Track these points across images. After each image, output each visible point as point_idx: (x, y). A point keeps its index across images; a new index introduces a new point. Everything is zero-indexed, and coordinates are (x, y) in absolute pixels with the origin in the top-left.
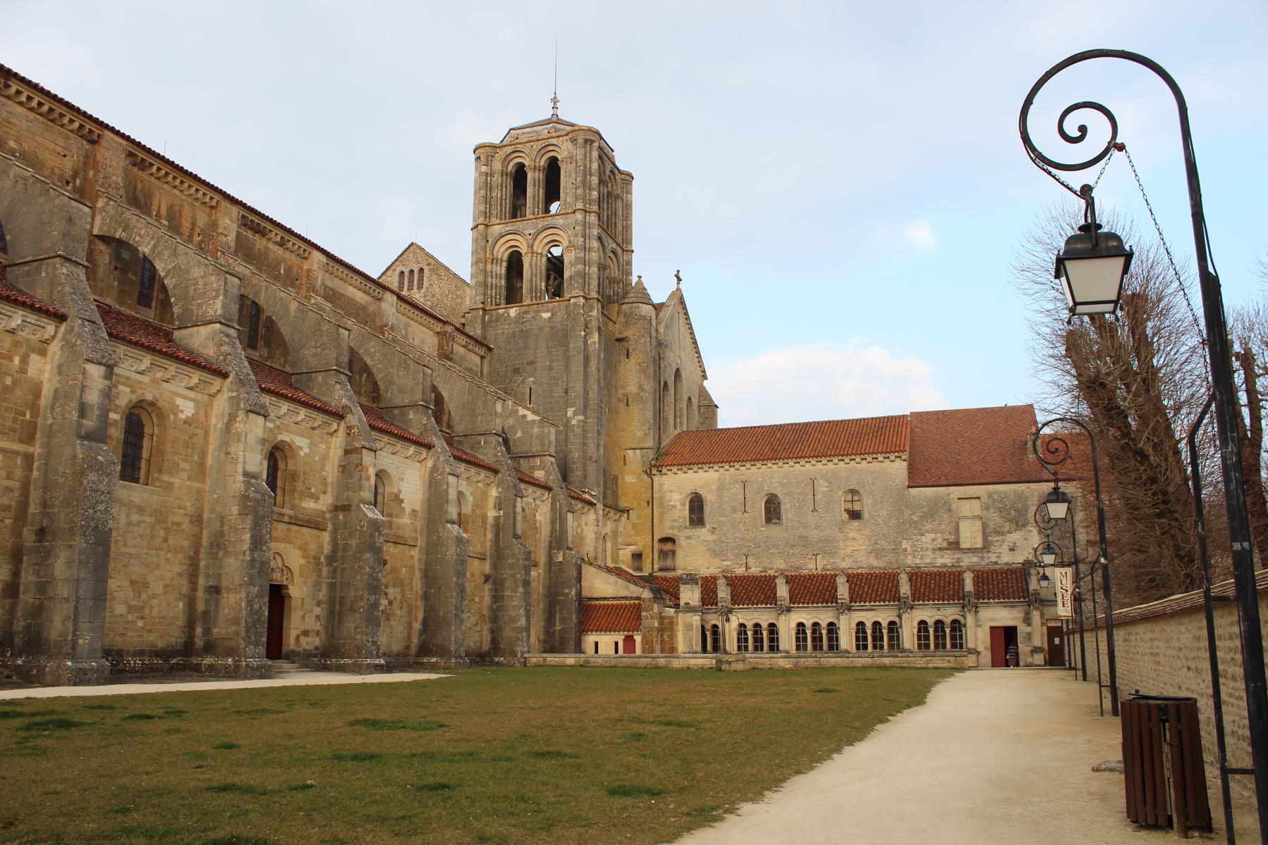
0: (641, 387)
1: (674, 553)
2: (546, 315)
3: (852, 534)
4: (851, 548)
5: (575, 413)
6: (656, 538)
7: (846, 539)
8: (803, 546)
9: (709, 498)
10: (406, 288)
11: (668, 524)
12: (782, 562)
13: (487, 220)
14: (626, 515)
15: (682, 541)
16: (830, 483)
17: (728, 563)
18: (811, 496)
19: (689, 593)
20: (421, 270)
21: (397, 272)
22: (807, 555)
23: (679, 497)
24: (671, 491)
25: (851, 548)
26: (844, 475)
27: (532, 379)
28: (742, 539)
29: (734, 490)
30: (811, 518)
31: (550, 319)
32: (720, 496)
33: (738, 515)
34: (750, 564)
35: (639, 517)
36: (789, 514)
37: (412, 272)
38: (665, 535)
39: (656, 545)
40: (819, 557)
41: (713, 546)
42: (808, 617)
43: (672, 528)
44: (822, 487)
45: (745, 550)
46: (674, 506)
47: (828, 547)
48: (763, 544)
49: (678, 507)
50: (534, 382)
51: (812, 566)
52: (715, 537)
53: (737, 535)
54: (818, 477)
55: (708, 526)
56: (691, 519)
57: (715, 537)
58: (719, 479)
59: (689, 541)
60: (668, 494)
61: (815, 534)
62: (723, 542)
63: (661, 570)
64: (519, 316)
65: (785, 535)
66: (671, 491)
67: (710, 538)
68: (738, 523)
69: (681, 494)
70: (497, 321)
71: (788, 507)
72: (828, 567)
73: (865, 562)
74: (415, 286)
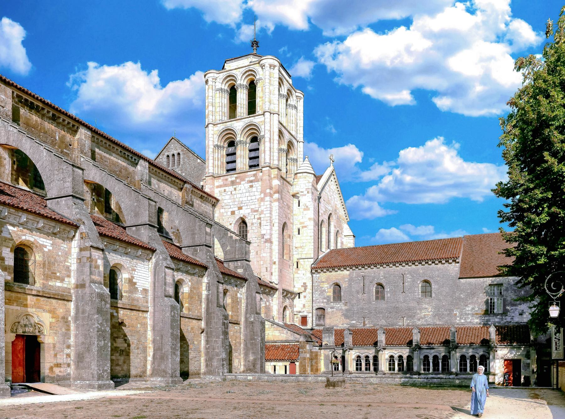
1: (324, 316)
3: (424, 306)
4: (424, 313)
6: (314, 308)
7: (421, 309)
9: (344, 286)
10: (170, 165)
14: (298, 296)
17: (354, 322)
18: (401, 284)
20: (179, 154)
22: (398, 317)
24: (323, 282)
25: (424, 313)
30: (401, 297)
33: (360, 296)
37: (173, 155)
39: (314, 311)
43: (323, 302)
44: (408, 279)
47: (410, 313)
49: (327, 291)
51: (400, 324)
52: (347, 307)
56: (334, 298)
57: (347, 307)
58: (349, 275)
59: (333, 310)
63: (317, 325)
67: (344, 308)
68: (360, 299)
71: (388, 290)
73: (432, 321)
74: (176, 164)
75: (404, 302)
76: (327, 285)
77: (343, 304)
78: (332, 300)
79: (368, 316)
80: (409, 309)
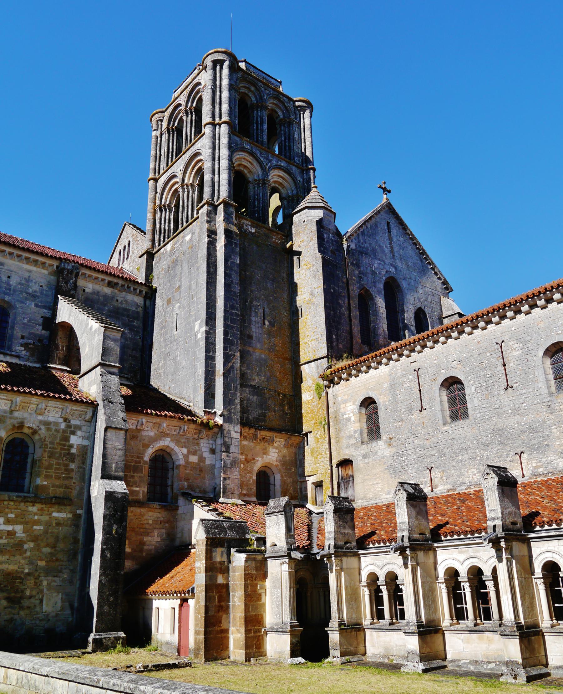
0: (312, 294)
2: (188, 238)
5: (200, 327)
8: (500, 443)
11: (344, 442)
12: (475, 471)
13: (157, 174)
15: (358, 463)
16: (524, 342)
18: (501, 368)
19: (275, 527)
21: (118, 253)
22: (507, 456)
23: (352, 407)
26: (542, 325)
27: (178, 304)
28: (423, 447)
29: (407, 384)
31: (191, 239)
32: (394, 395)
34: (436, 481)
35: (317, 441)
36: (476, 402)
38: (342, 457)
40: (524, 456)
41: (391, 462)
42: (462, 557)
43: (348, 447)
45: (427, 462)
46: (349, 419)
48: (448, 450)
49: (353, 419)
50: (180, 307)
52: (392, 450)
53: (418, 442)
54: (506, 338)
55: (384, 436)
57: (392, 450)
58: (390, 374)
59: (366, 460)
60: (342, 406)
61: (514, 422)
62: (401, 455)
64: (173, 248)
65: (475, 432)
66: (345, 402)
69: (354, 404)
70: (160, 260)
72: (541, 470)
75: (516, 411)
76: (352, 407)
77: (385, 442)
78: (366, 438)
79: (438, 463)
80: (531, 429)
